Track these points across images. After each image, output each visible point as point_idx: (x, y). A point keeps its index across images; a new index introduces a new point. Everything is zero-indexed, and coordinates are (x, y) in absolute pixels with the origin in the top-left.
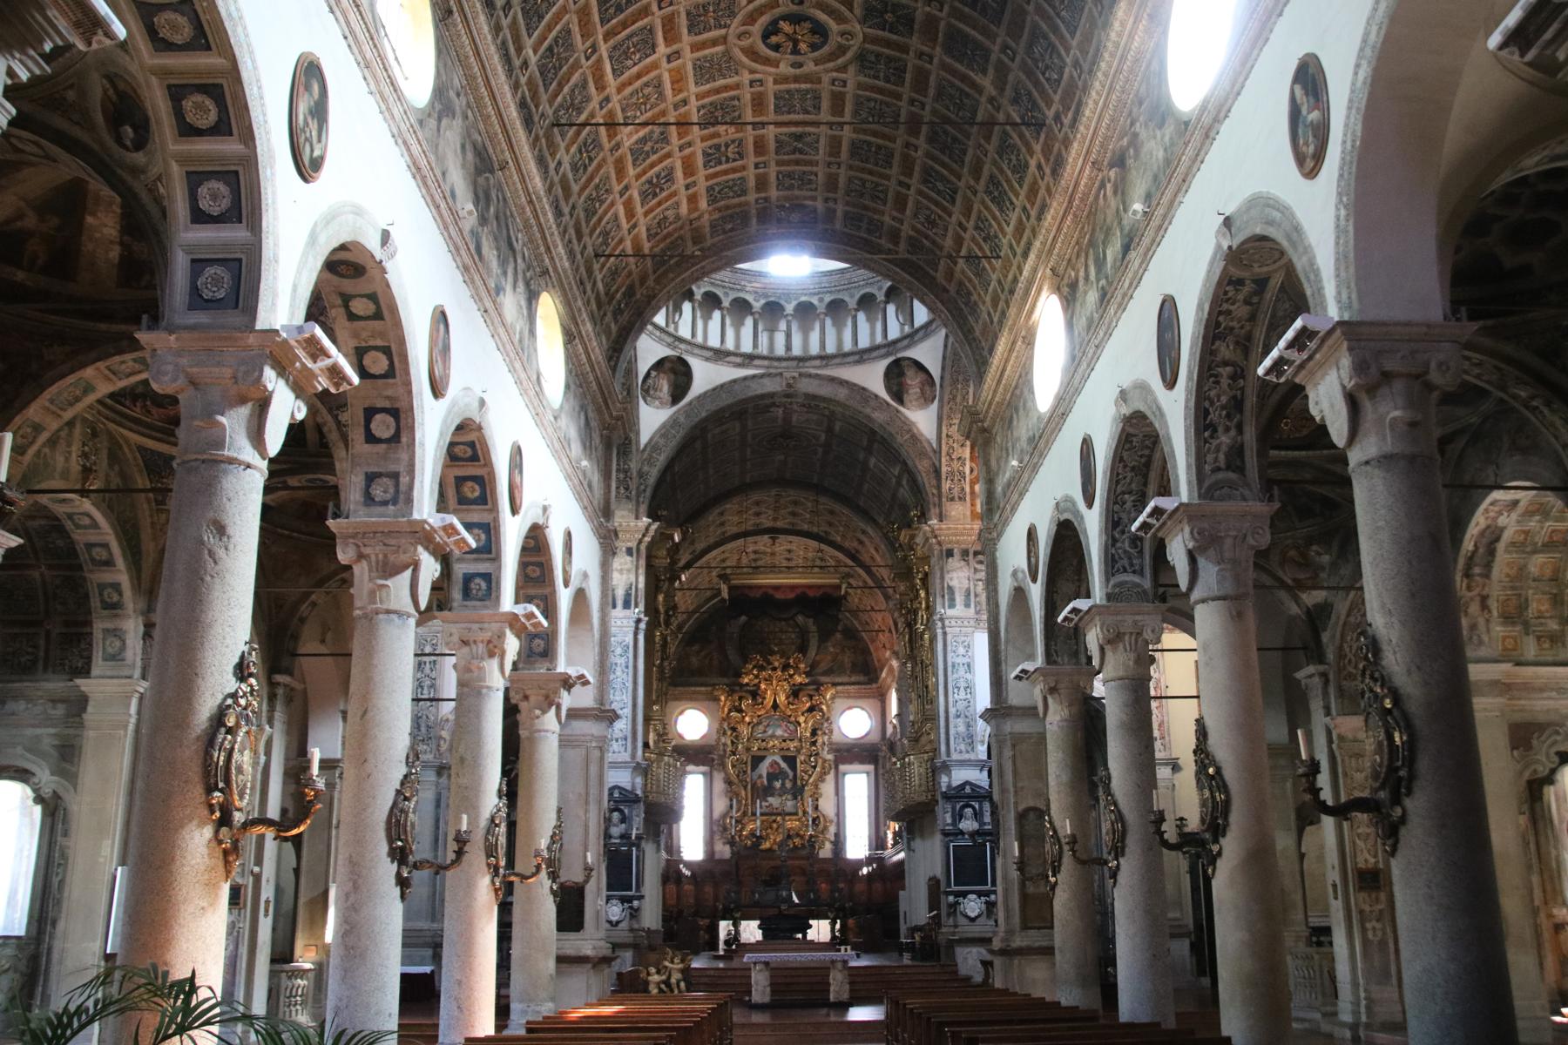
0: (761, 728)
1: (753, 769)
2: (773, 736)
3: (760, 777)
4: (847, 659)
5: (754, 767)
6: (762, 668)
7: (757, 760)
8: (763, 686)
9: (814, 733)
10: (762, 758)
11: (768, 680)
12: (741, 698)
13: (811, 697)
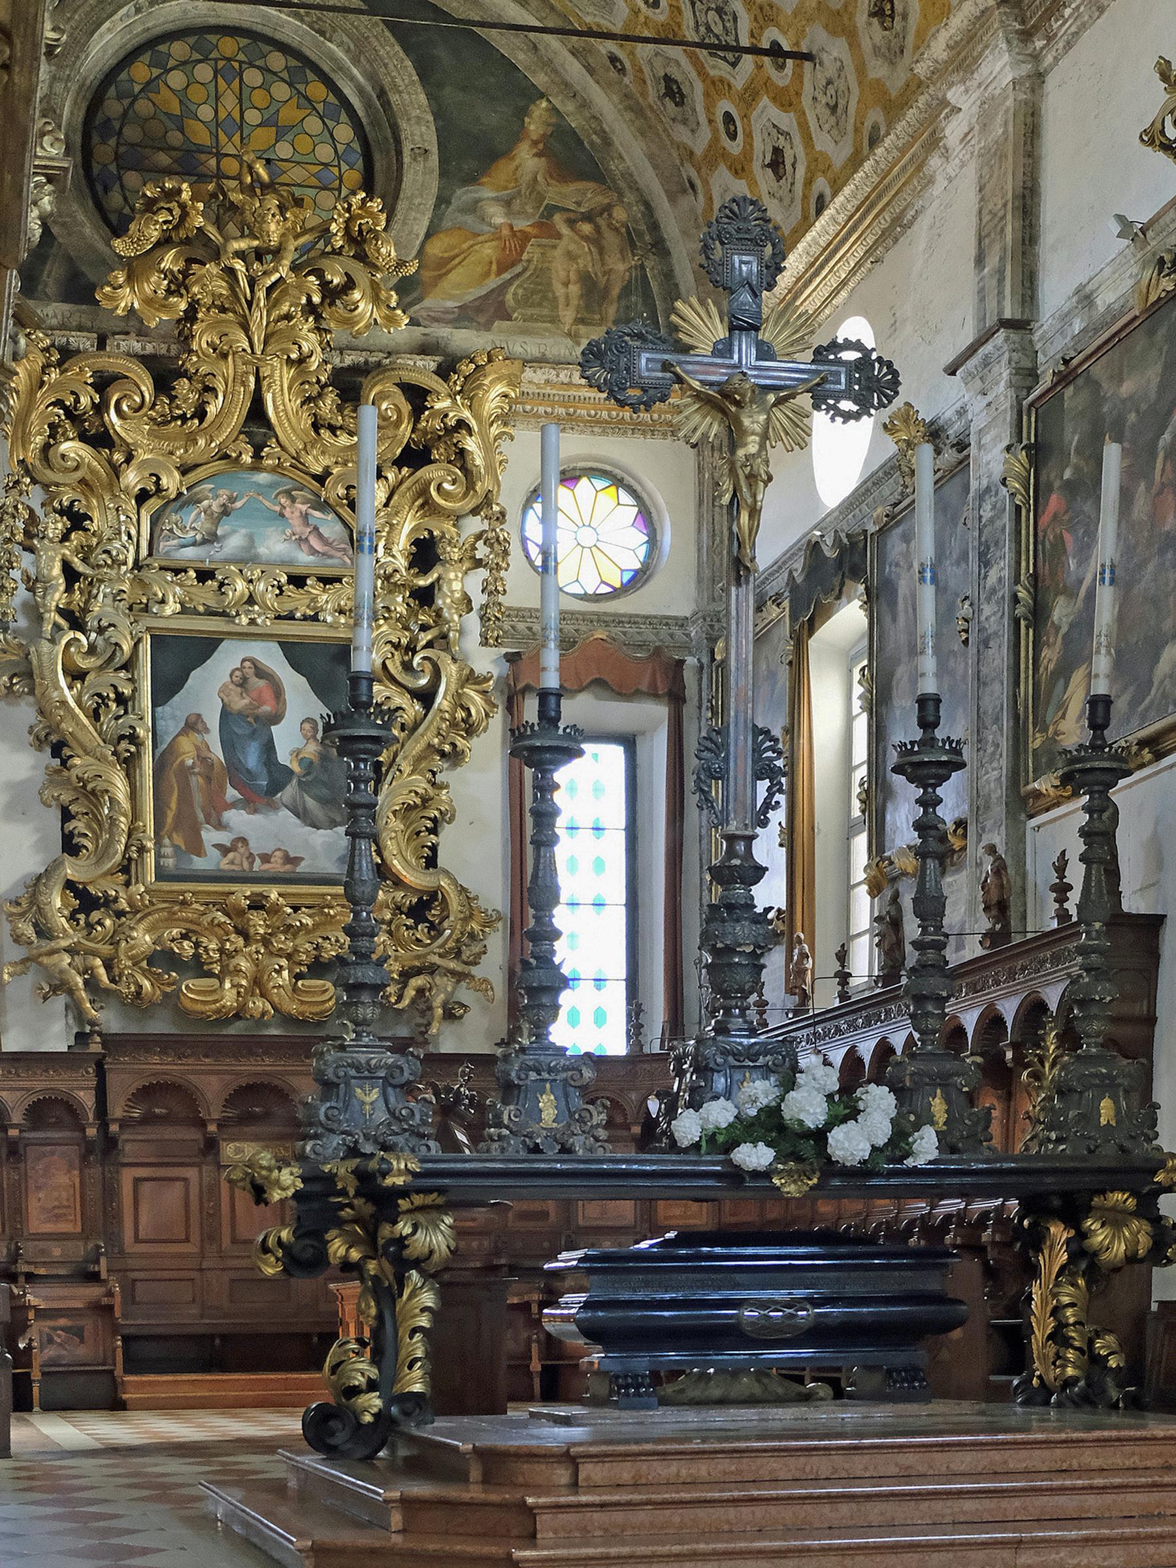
0: (194, 521)
1: (167, 687)
2: (247, 559)
3: (193, 725)
4: (565, 260)
5: (167, 687)
6: (201, 249)
7: (180, 656)
8: (202, 340)
9: (425, 554)
10: (203, 648)
11: (235, 307)
12: (103, 383)
13: (417, 396)
